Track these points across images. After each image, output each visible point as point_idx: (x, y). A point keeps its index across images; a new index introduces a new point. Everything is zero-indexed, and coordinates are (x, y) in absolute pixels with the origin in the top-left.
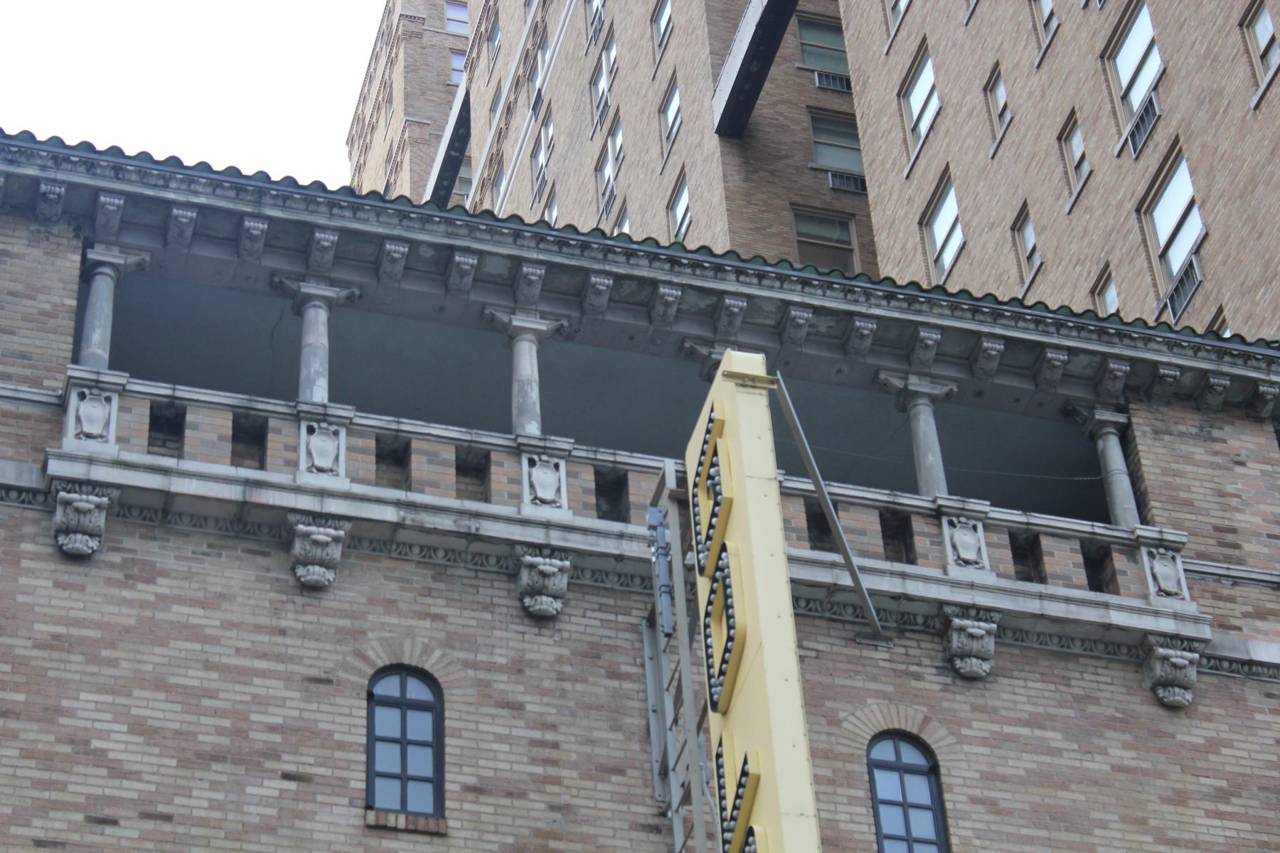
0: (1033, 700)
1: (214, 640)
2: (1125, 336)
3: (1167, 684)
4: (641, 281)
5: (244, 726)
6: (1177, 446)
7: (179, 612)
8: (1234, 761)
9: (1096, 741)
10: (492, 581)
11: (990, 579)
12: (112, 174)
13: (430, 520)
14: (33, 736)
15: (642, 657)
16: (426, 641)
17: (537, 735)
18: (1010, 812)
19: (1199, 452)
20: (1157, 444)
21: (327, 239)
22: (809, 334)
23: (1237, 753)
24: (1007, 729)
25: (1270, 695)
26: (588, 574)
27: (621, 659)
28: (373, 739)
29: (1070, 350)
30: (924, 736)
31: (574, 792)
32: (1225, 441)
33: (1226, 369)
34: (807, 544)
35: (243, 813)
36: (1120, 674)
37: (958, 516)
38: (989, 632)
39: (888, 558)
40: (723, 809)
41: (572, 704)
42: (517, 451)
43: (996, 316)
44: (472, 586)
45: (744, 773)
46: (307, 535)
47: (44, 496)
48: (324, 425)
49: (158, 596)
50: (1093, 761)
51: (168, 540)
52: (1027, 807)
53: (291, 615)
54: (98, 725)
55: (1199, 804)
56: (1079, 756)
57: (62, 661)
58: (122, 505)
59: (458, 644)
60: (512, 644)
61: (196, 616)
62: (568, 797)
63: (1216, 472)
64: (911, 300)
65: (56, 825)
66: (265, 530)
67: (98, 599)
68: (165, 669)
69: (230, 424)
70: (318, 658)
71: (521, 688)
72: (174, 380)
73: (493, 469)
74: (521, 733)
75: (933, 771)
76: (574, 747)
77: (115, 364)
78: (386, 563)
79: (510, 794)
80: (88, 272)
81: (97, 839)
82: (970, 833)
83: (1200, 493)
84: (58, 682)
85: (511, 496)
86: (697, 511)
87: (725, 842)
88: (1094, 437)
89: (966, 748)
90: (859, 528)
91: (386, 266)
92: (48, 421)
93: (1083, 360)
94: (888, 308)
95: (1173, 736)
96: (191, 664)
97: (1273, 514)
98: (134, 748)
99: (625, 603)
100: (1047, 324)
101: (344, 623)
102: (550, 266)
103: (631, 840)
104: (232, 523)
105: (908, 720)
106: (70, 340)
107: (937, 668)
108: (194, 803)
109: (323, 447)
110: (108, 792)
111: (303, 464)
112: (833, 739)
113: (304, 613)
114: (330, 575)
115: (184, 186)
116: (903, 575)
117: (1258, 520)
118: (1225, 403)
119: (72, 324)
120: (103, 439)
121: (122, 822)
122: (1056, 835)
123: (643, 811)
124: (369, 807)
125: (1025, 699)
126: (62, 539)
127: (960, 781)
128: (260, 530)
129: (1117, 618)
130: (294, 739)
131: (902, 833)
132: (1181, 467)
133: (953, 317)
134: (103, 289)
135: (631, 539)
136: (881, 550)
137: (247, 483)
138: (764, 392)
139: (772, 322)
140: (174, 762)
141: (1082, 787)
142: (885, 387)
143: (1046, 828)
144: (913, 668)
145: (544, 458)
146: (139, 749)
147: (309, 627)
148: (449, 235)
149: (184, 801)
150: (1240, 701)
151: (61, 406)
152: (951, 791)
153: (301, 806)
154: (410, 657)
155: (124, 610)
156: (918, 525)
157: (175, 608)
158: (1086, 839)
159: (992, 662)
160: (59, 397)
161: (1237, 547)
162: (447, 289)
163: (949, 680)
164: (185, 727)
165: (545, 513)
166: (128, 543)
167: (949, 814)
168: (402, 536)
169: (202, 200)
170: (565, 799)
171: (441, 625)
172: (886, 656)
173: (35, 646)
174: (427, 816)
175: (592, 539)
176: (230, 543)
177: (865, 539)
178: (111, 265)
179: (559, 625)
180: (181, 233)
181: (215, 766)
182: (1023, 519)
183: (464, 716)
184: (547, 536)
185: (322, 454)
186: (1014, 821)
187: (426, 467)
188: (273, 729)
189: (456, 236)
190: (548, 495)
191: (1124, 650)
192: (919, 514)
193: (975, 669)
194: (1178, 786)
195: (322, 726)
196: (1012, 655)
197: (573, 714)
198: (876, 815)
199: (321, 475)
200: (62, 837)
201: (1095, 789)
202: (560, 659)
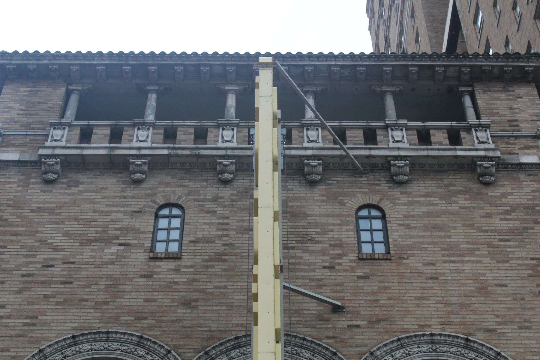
1: (99, 203)
3: (483, 175)
5: (106, 229)
7: (86, 195)
8: (513, 200)
9: (453, 199)
13: (180, 152)
14: (26, 241)
17: (221, 221)
18: (415, 228)
19: (503, 96)
20: (485, 95)
23: (514, 197)
24: (415, 199)
25: (530, 175)
29: (445, 66)
30: (379, 205)
31: (234, 239)
33: (510, 64)
39: (365, 145)
41: (235, 209)
46: (133, 163)
49: (79, 191)
50: (452, 206)
52: (422, 225)
54: (51, 235)
57: (40, 215)
60: (213, 192)
61: (92, 196)
63: (510, 102)
65: (31, 269)
70: (137, 204)
71: (216, 206)
74: (214, 221)
75: (383, 217)
76: (235, 224)
79: (208, 242)
81: (46, 272)
82: (397, 237)
89: (397, 207)
95: (487, 194)
96: (89, 211)
98: (64, 241)
105: (374, 200)
108: (84, 257)
110: (52, 256)
111: (135, 139)
112: (341, 210)
117: (527, 116)
121: (56, 266)
129: (460, 153)
130: (125, 232)
139: (327, 75)
143: (430, 232)
146: (65, 241)
147: (135, 195)
148: (198, 61)
149: (81, 257)
153: (125, 254)
154: (173, 200)
155: (66, 197)
157: (85, 194)
161: (518, 126)
163: (391, 185)
164: (84, 232)
166: (70, 175)
167: (389, 231)
168: (172, 160)
169: (107, 62)
171: (186, 188)
172: (366, 179)
173: (31, 212)
175: (244, 151)
177: (356, 139)
179: (233, 183)
181: (93, 244)
182: (422, 124)
183: (192, 218)
185: (142, 136)
188: (117, 229)
194: (488, 211)
200: (32, 273)
202: (232, 195)
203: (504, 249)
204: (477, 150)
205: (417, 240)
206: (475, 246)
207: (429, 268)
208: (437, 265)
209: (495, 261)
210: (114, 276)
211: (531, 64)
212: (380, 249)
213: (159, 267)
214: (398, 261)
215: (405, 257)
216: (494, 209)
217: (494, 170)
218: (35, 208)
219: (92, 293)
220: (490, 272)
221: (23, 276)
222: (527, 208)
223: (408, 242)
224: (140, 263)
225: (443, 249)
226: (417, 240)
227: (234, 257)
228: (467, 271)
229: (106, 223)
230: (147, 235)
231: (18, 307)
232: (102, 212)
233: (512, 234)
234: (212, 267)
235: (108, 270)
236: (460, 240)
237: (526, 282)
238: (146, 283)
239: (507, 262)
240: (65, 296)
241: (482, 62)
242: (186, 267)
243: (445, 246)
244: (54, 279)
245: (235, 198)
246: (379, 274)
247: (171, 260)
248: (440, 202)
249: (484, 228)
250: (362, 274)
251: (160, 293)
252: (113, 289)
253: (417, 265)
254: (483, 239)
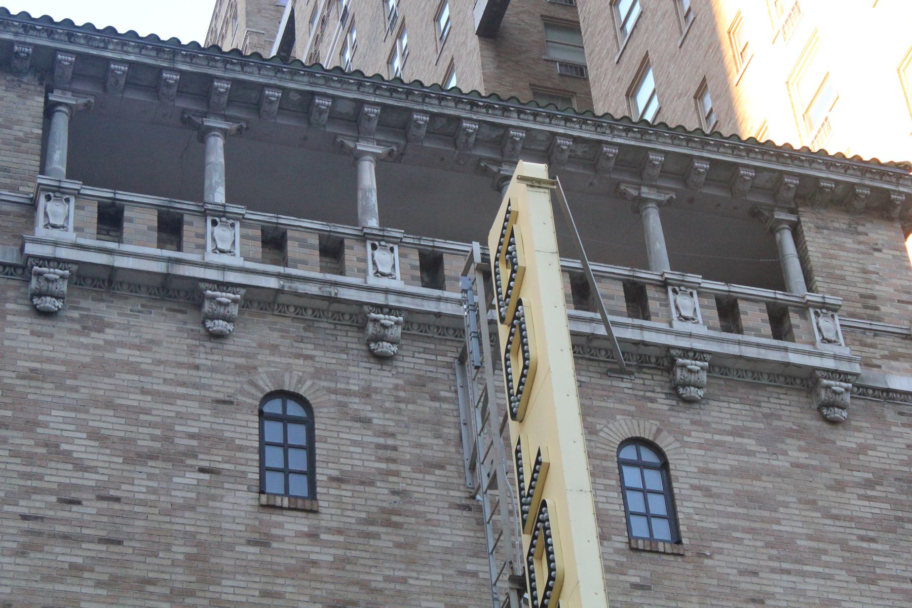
0: (734, 417)
2: (796, 158)
3: (829, 405)
4: (449, 117)
5: (170, 434)
9: (780, 446)
10: (347, 331)
11: (702, 330)
12: (66, 39)
13: (302, 288)
14: (19, 441)
15: (456, 386)
16: (300, 374)
17: (381, 441)
18: (719, 496)
20: (818, 235)
21: (223, 86)
22: (569, 157)
25: (902, 414)
26: (415, 327)
27: (441, 387)
28: (263, 444)
29: (756, 168)
30: (657, 442)
31: (409, 481)
32: (867, 234)
33: (867, 182)
34: (573, 306)
35: (171, 496)
36: (796, 398)
37: (679, 286)
38: (702, 368)
40: (521, 489)
41: (406, 419)
42: (363, 238)
43: (704, 144)
44: (332, 335)
45: (538, 462)
46: (213, 298)
47: (23, 269)
48: (224, 219)
49: (106, 341)
50: (777, 460)
51: (112, 302)
52: (732, 492)
53: (202, 356)
54: (65, 434)
55: (853, 490)
56: (768, 457)
58: (79, 276)
59: (323, 377)
60: (362, 376)
61: (134, 356)
62: (404, 485)
63: (861, 256)
64: (643, 132)
65: (36, 504)
66: (182, 294)
67: (63, 344)
68: (112, 394)
69: (156, 218)
71: (369, 408)
72: (115, 187)
73: (346, 251)
75: (664, 467)
76: (408, 450)
77: (70, 175)
78: (270, 319)
79: (362, 483)
80: (50, 110)
81: (66, 514)
82: (692, 511)
83: (850, 271)
84: (35, 402)
85: (359, 270)
86: (498, 279)
87: (523, 512)
88: (773, 232)
89: (687, 450)
90: (612, 294)
91: (266, 106)
92: (23, 216)
93: (766, 176)
94: (627, 138)
95: (834, 442)
96: (131, 390)
99: (442, 347)
100: (740, 150)
101: (241, 361)
102: (384, 107)
103: (450, 516)
104: (158, 289)
106: (38, 158)
107: (666, 394)
108: (136, 489)
109: (224, 235)
110: (74, 481)
111: (210, 247)
112: (592, 444)
113: (212, 354)
114: (230, 327)
115: (119, 48)
116: (642, 328)
117: (891, 290)
118: (867, 207)
119: (39, 147)
120: (63, 228)
122: (753, 512)
123: (458, 495)
124: (262, 492)
125: (728, 416)
126: (36, 301)
127: (684, 474)
128: (179, 294)
129: (794, 358)
130: (207, 444)
131: (643, 510)
132: (836, 252)
133: (673, 144)
134: (61, 122)
135: (447, 302)
136: (625, 310)
137: (170, 260)
138: (547, 191)
139: (543, 148)
140: (120, 460)
141: (771, 479)
142: (624, 194)
144: (649, 394)
145: (383, 243)
146: (95, 450)
149: (129, 488)
150: (880, 418)
151: (33, 205)
152: (678, 481)
153: (213, 491)
154: (289, 385)
155: (82, 351)
156: (651, 292)
157: (119, 350)
158: (774, 515)
159: (705, 390)
160: (31, 199)
161: (877, 309)
162: (310, 124)
163: (674, 403)
164: (128, 435)
165: (384, 283)
166: (84, 304)
167: (677, 497)
168: (282, 299)
169: (132, 58)
170: (402, 486)
171: (310, 362)
172: (630, 385)
173: (18, 378)
174: (303, 498)
175: (418, 301)
176: (158, 304)
177: (613, 302)
178: (66, 105)
179: (396, 363)
180: (117, 82)
181: (150, 463)
182: (726, 288)
183: (329, 428)
184: (386, 299)
185: (223, 240)
186: (722, 502)
187: (298, 250)
188: (192, 436)
189: (316, 84)
190: (386, 270)
191: (798, 381)
192: (651, 284)
193: (693, 394)
194: (838, 477)
195: (227, 434)
196: (719, 385)
197: (406, 427)
198: (624, 498)
199: (222, 255)
200: (41, 513)
201: (779, 480)
202: (396, 387)
203: (868, 557)
205: (724, 521)
207: (748, 579)
208: (761, 575)
209: (854, 579)
210: (198, 537)
211: (902, 189)
212: (662, 530)
213: (280, 525)
214: (696, 559)
215: (708, 554)
218: (26, 370)
219: (161, 569)
221: (25, 517)
222: (900, 480)
223: (710, 524)
224: (243, 514)
225: (768, 545)
226: (724, 521)
227: (413, 520)
229: (169, 420)
230: (250, 456)
231: (23, 584)
232: (158, 393)
233: (879, 528)
234: (376, 536)
235: (185, 521)
236: (796, 530)
238: (260, 558)
239: (873, 582)
240: (111, 570)
241: (820, 170)
242: (329, 530)
243: (772, 539)
244: (85, 531)
245: (402, 394)
246: (666, 583)
247: (299, 514)
250: (637, 580)
251: (288, 582)
252: (200, 565)
253: (729, 571)
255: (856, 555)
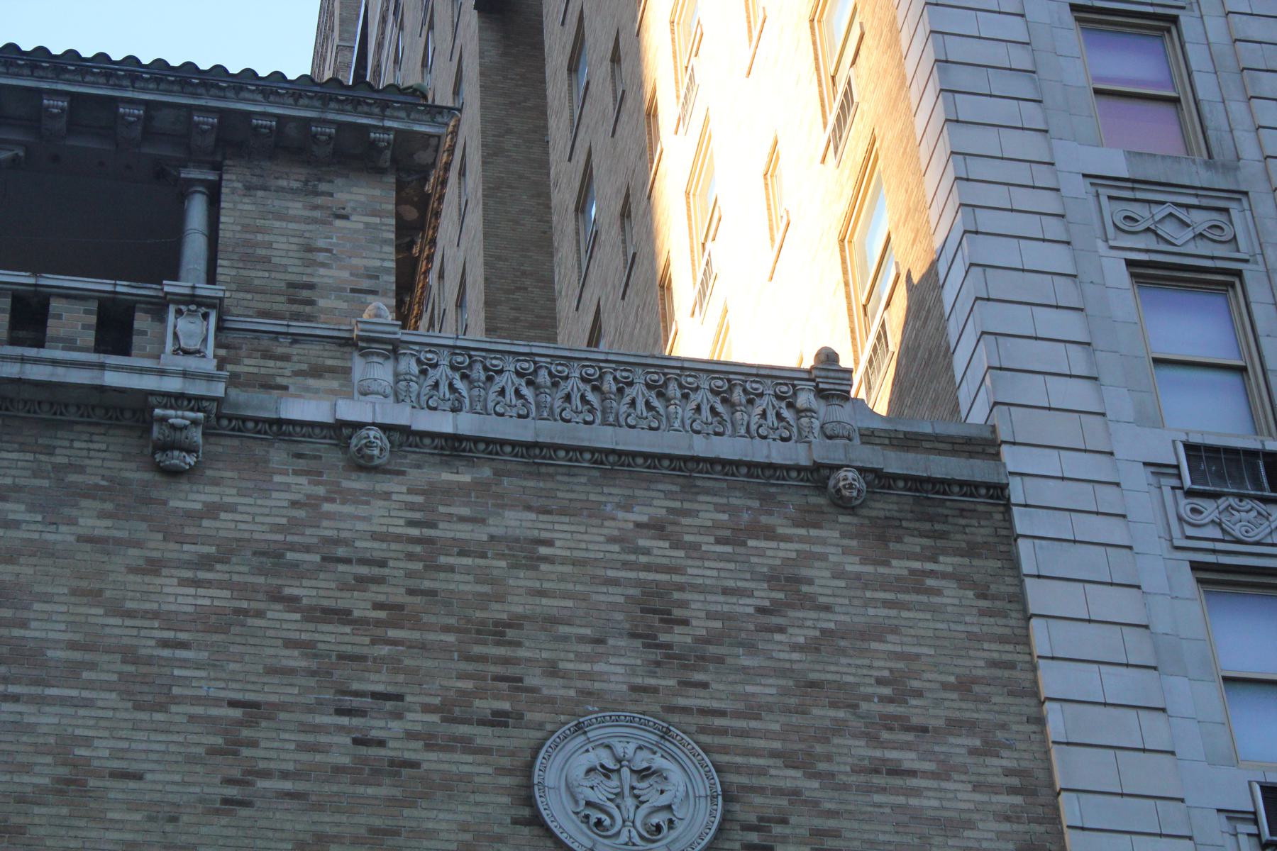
2: (212, 86)
3: (165, 447)
6: (269, 202)
8: (232, 525)
9: (66, 511)
19: (296, 207)
20: (246, 200)
23: (238, 517)
25: (299, 456)
32: (331, 195)
50: (56, 532)
56: (40, 527)
95: (165, 503)
97: (366, 268)
100: (118, 77)
117: (345, 274)
141: (33, 560)
161: (311, 303)
182: (32, 281)
191: (128, 414)
194: (155, 554)
203: (167, 670)
204: (162, 372)
206: (88, 657)
211: (388, 123)
216: (171, 550)
217: (197, 435)
220: (106, 734)
222: (263, 554)
228: (45, 729)
233: (200, 627)
236: (51, 635)
237: (198, 768)
239: (162, 708)
241: (254, 102)
248: (28, 517)
249: (130, 605)
254: (116, 636)
255: (144, 669)
